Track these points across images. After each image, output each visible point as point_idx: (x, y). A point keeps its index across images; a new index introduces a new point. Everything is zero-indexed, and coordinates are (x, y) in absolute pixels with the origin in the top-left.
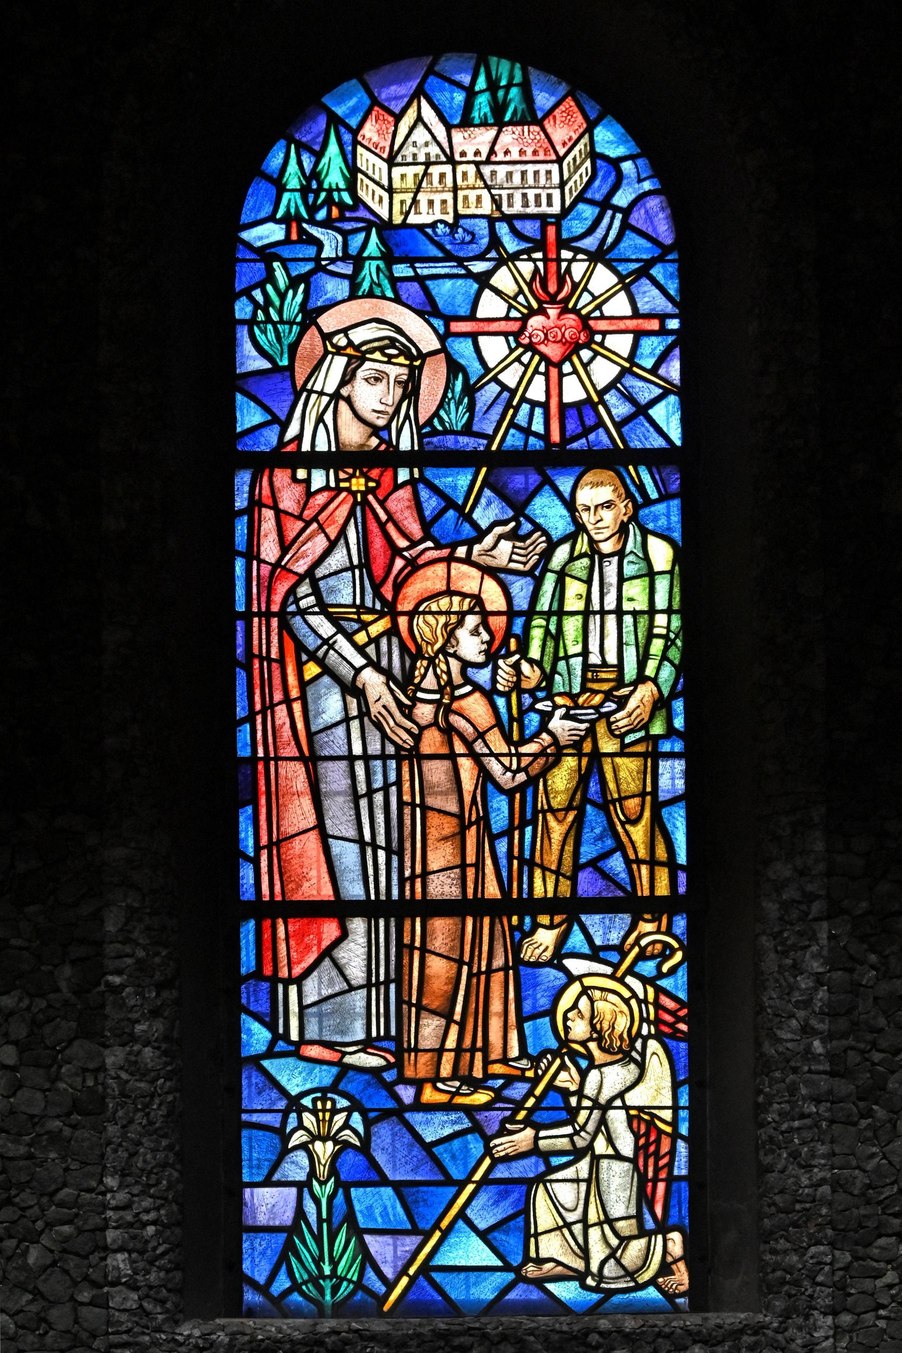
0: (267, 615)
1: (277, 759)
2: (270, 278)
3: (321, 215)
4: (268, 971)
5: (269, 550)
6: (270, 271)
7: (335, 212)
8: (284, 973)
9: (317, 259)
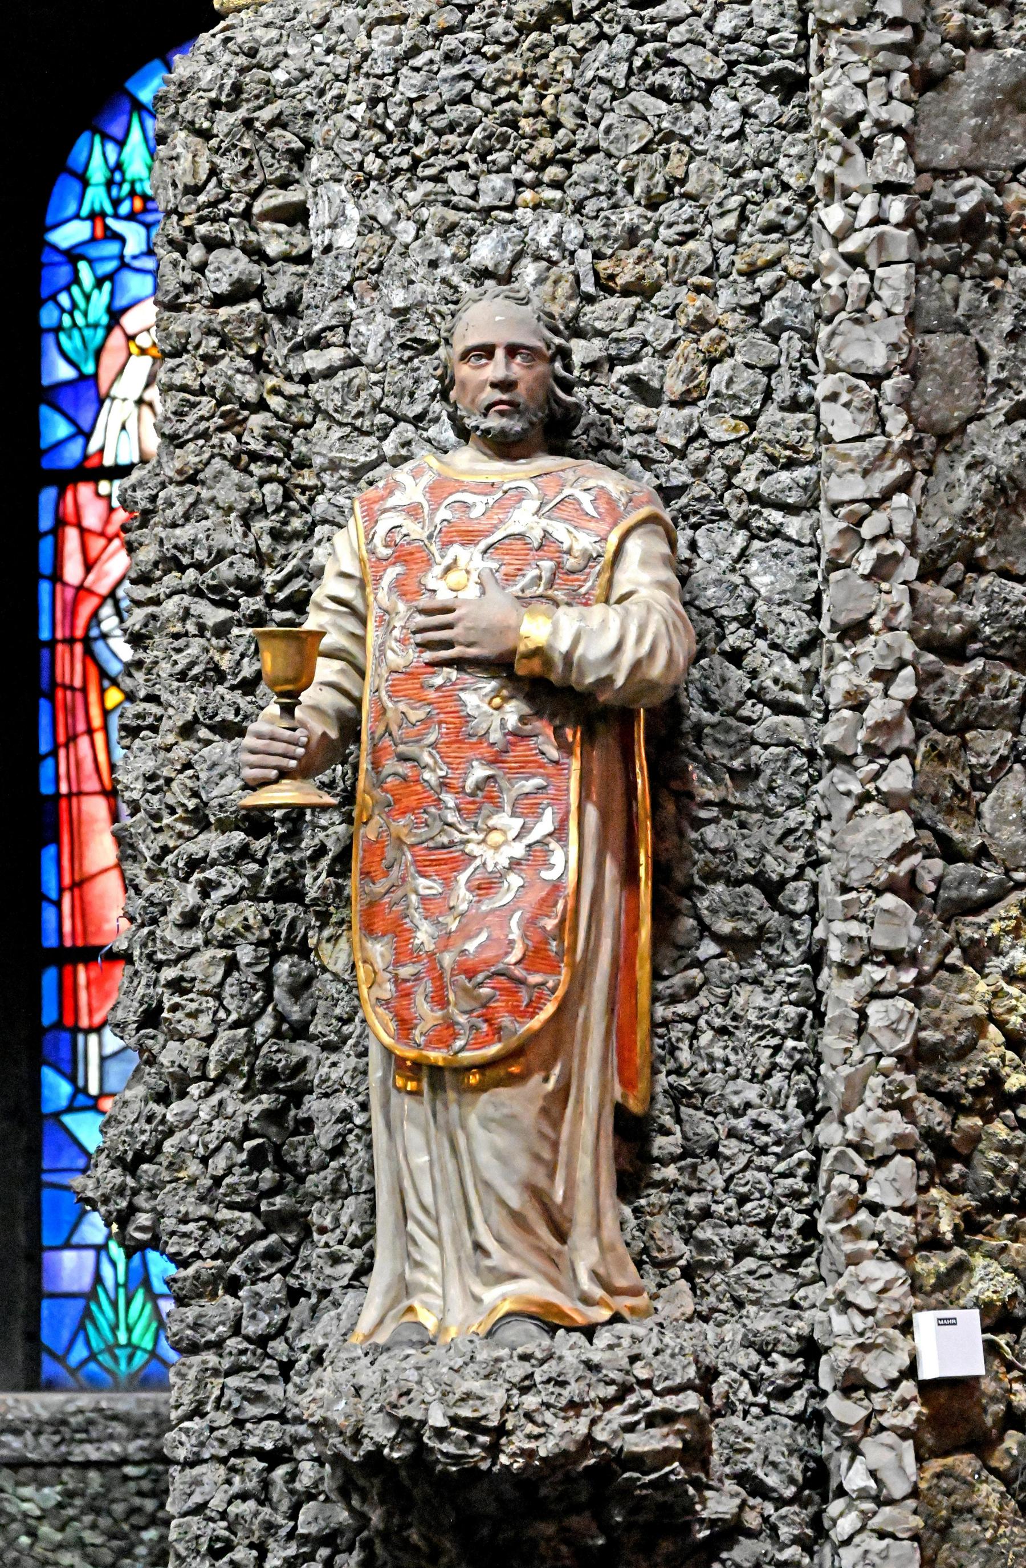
0: (70, 641)
1: (80, 794)
2: (76, 280)
3: (124, 209)
4: (68, 1021)
5: (73, 571)
6: (76, 272)
7: (138, 204)
8: (84, 1022)
9: (121, 257)
